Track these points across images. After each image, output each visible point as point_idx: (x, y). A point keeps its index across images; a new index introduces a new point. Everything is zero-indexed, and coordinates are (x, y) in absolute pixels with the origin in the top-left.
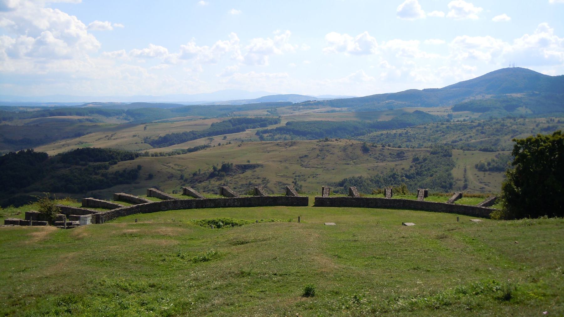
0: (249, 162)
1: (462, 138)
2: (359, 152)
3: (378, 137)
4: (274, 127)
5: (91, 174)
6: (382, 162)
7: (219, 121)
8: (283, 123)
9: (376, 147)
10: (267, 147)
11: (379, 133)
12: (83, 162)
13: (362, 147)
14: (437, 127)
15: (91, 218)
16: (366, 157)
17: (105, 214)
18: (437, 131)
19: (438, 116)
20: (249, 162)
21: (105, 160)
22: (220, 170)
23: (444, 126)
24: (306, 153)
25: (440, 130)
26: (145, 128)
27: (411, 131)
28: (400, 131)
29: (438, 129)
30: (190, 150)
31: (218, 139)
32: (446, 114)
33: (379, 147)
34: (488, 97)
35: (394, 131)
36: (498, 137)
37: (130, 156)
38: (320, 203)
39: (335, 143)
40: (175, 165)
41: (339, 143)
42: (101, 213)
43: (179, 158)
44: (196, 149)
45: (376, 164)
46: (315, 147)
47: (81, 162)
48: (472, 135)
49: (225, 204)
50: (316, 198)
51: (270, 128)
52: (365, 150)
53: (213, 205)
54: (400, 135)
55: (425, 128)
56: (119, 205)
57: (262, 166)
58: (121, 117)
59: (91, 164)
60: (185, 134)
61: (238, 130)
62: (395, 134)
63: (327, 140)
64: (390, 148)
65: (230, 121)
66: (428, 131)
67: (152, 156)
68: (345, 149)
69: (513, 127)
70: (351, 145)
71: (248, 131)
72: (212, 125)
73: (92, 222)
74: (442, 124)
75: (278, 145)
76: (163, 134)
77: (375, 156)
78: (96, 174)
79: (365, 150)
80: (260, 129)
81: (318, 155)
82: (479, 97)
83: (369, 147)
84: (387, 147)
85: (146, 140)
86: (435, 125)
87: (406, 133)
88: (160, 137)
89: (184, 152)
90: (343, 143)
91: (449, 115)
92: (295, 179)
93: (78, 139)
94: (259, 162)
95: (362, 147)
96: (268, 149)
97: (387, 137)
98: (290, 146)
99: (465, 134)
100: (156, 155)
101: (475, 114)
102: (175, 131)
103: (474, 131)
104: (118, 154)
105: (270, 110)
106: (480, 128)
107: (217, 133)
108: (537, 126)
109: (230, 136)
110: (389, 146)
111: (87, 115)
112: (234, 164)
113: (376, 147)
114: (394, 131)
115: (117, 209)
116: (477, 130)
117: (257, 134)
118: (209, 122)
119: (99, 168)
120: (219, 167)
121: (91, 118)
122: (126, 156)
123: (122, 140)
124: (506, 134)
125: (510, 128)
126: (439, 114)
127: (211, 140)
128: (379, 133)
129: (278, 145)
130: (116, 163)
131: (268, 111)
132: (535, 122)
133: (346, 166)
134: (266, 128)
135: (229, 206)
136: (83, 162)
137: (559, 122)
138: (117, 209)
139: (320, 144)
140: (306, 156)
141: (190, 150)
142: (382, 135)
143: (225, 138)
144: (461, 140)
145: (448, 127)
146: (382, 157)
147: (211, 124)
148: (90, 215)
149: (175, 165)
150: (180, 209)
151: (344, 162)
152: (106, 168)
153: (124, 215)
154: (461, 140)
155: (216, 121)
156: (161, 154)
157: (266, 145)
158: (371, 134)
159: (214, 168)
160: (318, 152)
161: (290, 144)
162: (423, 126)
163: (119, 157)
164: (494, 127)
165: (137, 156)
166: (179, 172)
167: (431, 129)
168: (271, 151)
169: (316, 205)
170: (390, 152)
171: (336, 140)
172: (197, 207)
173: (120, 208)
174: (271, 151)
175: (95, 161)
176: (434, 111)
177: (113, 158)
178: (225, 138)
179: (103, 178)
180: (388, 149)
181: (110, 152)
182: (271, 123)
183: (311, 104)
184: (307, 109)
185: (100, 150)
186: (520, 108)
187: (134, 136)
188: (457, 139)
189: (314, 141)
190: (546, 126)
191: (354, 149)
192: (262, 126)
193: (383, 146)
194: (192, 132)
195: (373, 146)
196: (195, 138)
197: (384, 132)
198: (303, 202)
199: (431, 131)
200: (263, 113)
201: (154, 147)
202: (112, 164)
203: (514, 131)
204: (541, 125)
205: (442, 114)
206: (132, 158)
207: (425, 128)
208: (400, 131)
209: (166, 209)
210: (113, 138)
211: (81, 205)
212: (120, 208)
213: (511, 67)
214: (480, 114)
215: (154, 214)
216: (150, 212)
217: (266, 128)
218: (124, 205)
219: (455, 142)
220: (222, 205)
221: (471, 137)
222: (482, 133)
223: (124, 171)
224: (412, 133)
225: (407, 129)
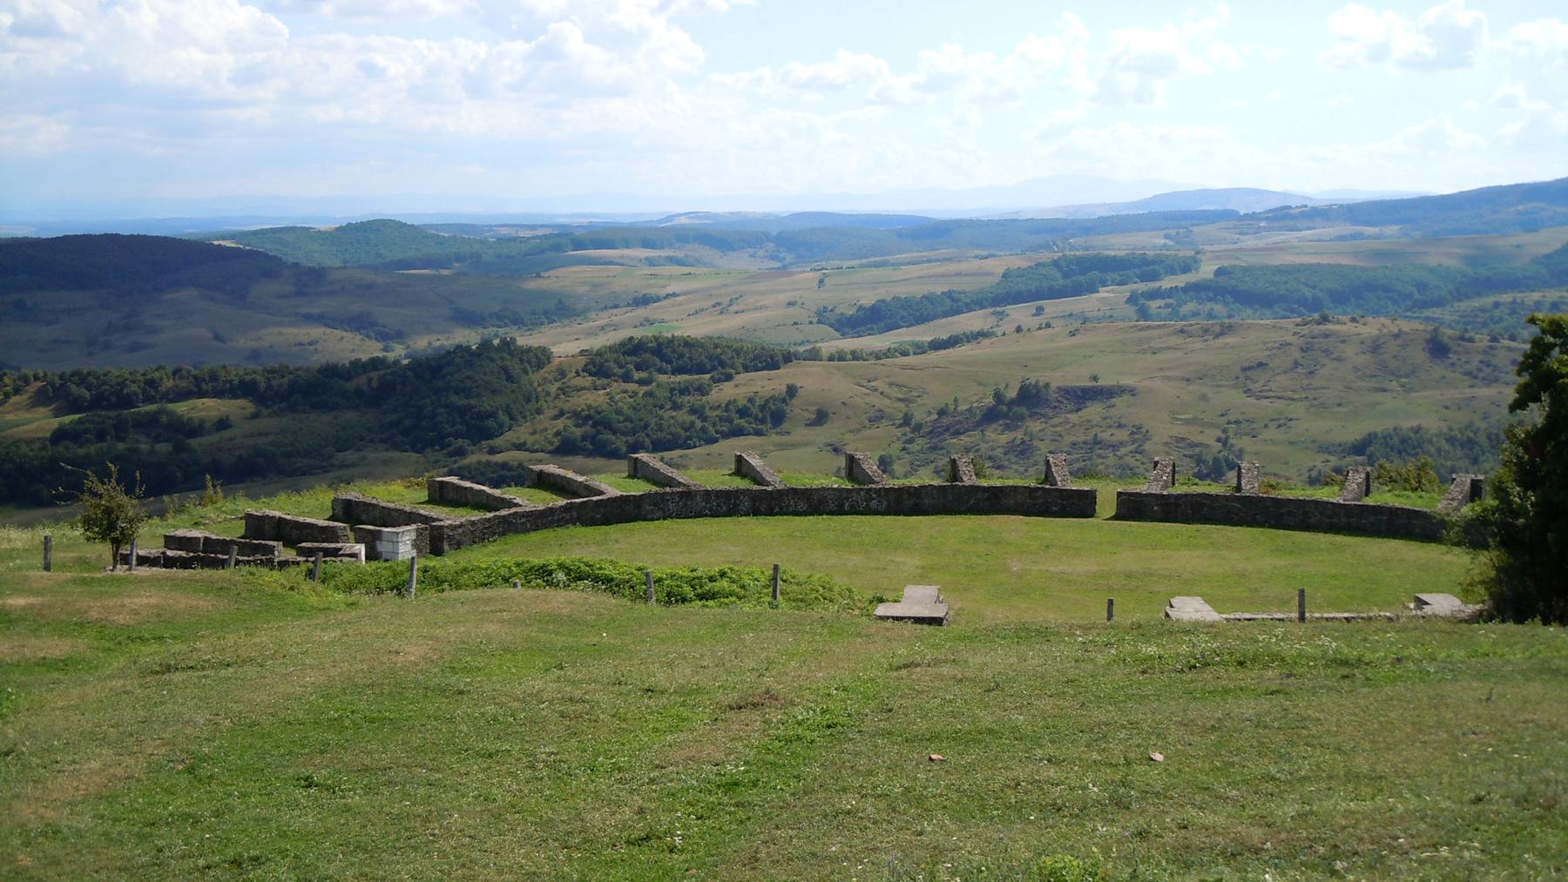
0: (1095, 378)
2: (1419, 356)
3: (1483, 310)
4: (1180, 281)
5: (662, 407)
6: (1488, 385)
7: (1025, 264)
8: (1206, 271)
9: (1471, 340)
10: (1151, 338)
11: (1489, 300)
12: (643, 375)
15: (413, 535)
16: (1439, 370)
17: (461, 525)
20: (1095, 378)
21: (701, 370)
22: (1012, 403)
24: (1261, 356)
26: (821, 281)
30: (937, 345)
31: (1020, 314)
33: (1483, 340)
35: (1536, 296)
37: (769, 360)
38: (1133, 508)
39: (1349, 328)
40: (891, 384)
42: (447, 523)
43: (904, 368)
44: (953, 342)
45: (1468, 392)
46: (1289, 338)
47: (637, 375)
49: (841, 506)
50: (1119, 494)
51: (1167, 283)
52: (1438, 349)
53: (802, 506)
56: (518, 501)
57: (1132, 392)
58: (761, 253)
59: (663, 378)
60: (929, 298)
61: (1077, 291)
62: (1538, 303)
63: (1325, 319)
64: (1513, 344)
65: (1056, 263)
67: (831, 359)
68: (1375, 347)
70: (1397, 336)
71: (1104, 293)
72: (1005, 276)
73: (415, 545)
75: (1182, 331)
76: (868, 299)
78: (676, 407)
79: (1438, 349)
80: (1142, 287)
81: (1296, 364)
83: (1451, 344)
84: (1506, 343)
85: (822, 316)
88: (860, 308)
89: (920, 349)
90: (1371, 328)
92: (1224, 431)
93: (641, 312)
94: (1126, 381)
95: (1428, 341)
96: (1155, 344)
97: (1513, 312)
98: (1218, 336)
100: (841, 358)
102: (903, 291)
104: (738, 352)
105: (1173, 232)
107: (1018, 298)
109: (1052, 307)
110: (1512, 338)
111: (671, 246)
112: (1053, 385)
113: (1471, 340)
114: (1536, 296)
115: (504, 512)
117: (1132, 300)
118: (997, 267)
119: (684, 391)
120: (1012, 394)
121: (680, 254)
122: (756, 358)
123: (757, 315)
127: (1001, 316)
128: (1489, 300)
129: (1182, 331)
130: (729, 378)
131: (1167, 237)
133: (1379, 397)
134: (1156, 285)
135: (854, 511)
136: (643, 375)
138: (504, 512)
139: (1305, 330)
140: (1261, 365)
141: (937, 345)
142: (1497, 305)
143: (1040, 310)
146: (1487, 371)
147: (1001, 270)
148: (414, 526)
149: (891, 384)
150: (699, 515)
151: (1373, 384)
152: (702, 390)
153: (526, 531)
155: (1017, 262)
156: (856, 356)
157: (1148, 333)
159: (998, 396)
160: (1297, 355)
161: (1218, 329)
163: (739, 362)
165: (788, 358)
166: (901, 405)
168: (1161, 350)
169: (1117, 517)
171: (1353, 320)
172: (756, 512)
173: (513, 510)
174: (1161, 350)
175: (675, 372)
177: (722, 364)
178: (1040, 310)
179: (693, 418)
180: (1509, 349)
181: (716, 346)
182: (1171, 271)
183: (1294, 217)
184: (1281, 229)
185: (688, 343)
187: (791, 304)
189: (1288, 323)
191: (1404, 346)
192: (1146, 278)
193: (1494, 339)
194: (949, 295)
195: (1462, 338)
196: (958, 312)
197: (1506, 298)
198: (1080, 505)
200: (1151, 242)
201: (844, 335)
202: (720, 380)
206: (774, 366)
209: (660, 513)
210: (734, 308)
211: (424, 495)
212: (513, 510)
215: (614, 530)
216: (607, 521)
217: (1156, 285)
218: (528, 500)
220: (833, 507)
223: (750, 400)
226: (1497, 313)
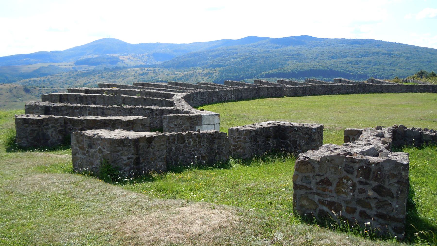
1: (90, 81)
2: (23, 93)
3: (27, 82)
9: (35, 88)
11: (27, 80)
13: (24, 89)
14: (70, 75)
16: (28, 95)
18: (71, 78)
19: (66, 69)
23: (74, 74)
25: (72, 77)
27: (52, 79)
28: (43, 78)
29: (71, 76)
32: (71, 67)
34: (96, 56)
36: (114, 80)
41: (4, 87)
48: (96, 79)
52: (27, 91)
54: (44, 81)
55: (61, 76)
62: (40, 80)
66: (64, 78)
68: (10, 91)
69: (122, 73)
70: (15, 88)
74: (73, 73)
77: (36, 94)
82: (90, 57)
83: (30, 89)
86: (68, 74)
87: (48, 79)
90: (7, 86)
91: (73, 68)
95: (24, 89)
97: (34, 83)
99: (91, 79)
101: (91, 66)
103: (96, 76)
106: (100, 75)
108: (136, 72)
110: (44, 87)
113: (35, 88)
116: (99, 76)
124: (118, 78)
125: (120, 74)
126: (66, 67)
132: (134, 70)
133: (14, 103)
137: (148, 70)
142: (30, 81)
144: (89, 82)
145: (77, 75)
151: (12, 100)
154: (89, 82)
158: (21, 81)
162: (59, 75)
164: (109, 74)
167: (65, 77)
170: (46, 91)
176: (63, 65)
180: (45, 90)
186: (119, 63)
188: (87, 82)
190: (141, 72)
191: (18, 90)
193: (40, 88)
197: (32, 79)
199: (66, 78)
203: (123, 76)
204: (138, 72)
205: (69, 67)
207: (61, 76)
208: (43, 78)
213: (108, 38)
214: (95, 67)
219: (86, 84)
221: (95, 80)
222: (103, 78)
224: (52, 79)
225: (48, 77)
226: (30, 83)
